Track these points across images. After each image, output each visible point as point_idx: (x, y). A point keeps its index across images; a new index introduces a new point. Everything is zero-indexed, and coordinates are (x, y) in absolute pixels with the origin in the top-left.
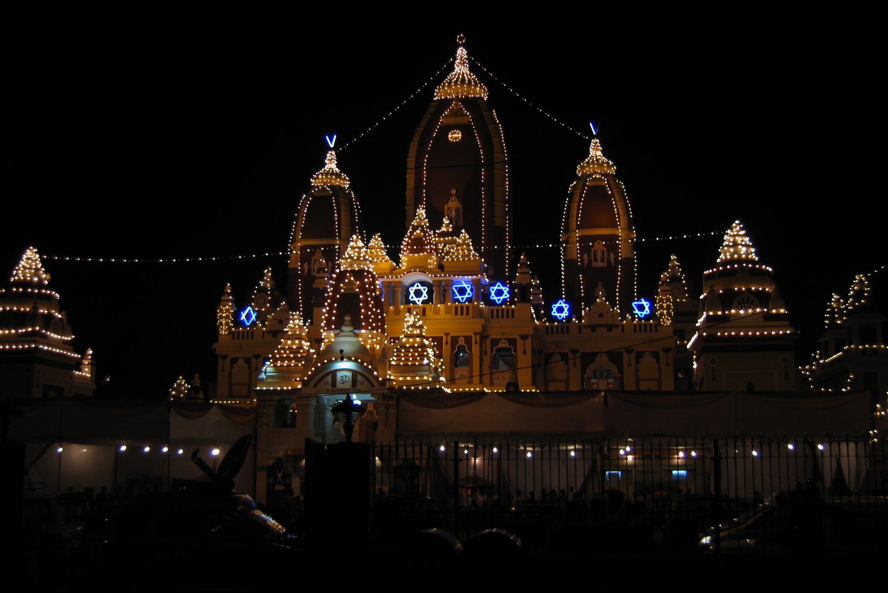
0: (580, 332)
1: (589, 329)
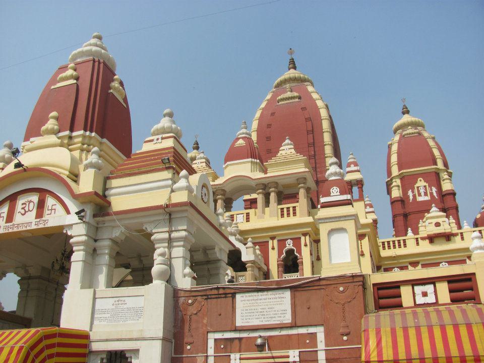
0: (418, 244)
1: (427, 241)
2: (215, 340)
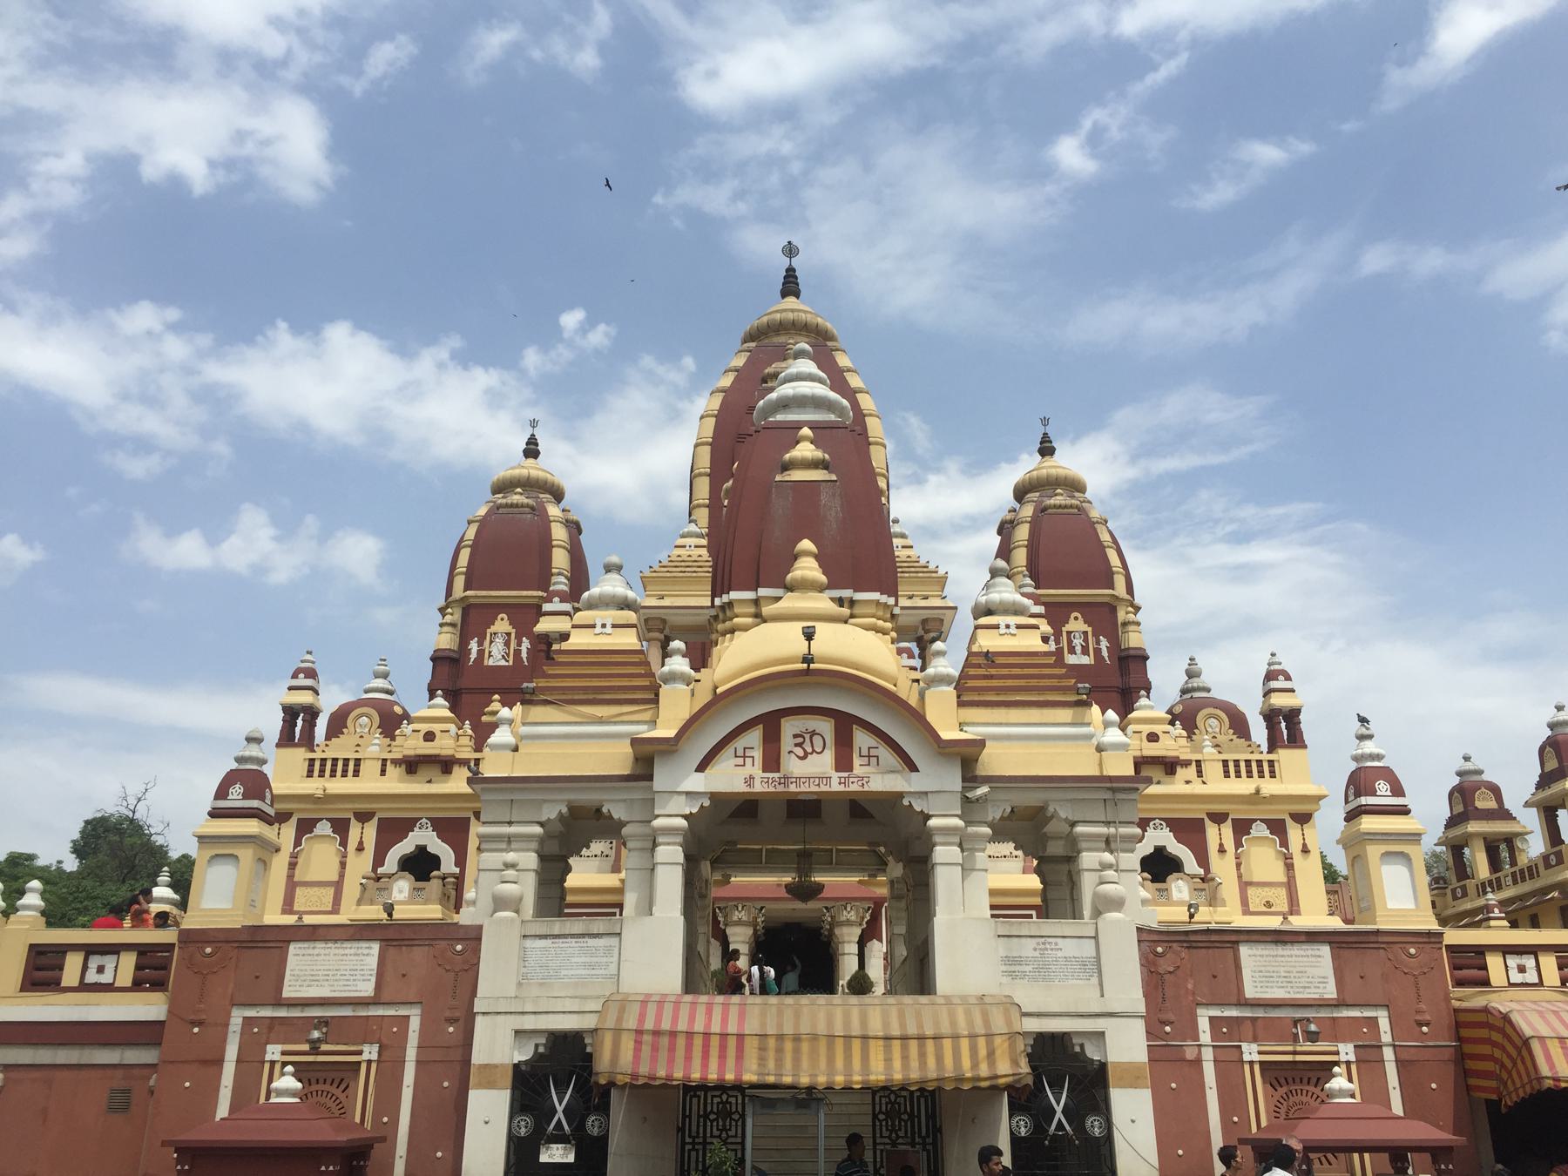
2: (1211, 1018)
